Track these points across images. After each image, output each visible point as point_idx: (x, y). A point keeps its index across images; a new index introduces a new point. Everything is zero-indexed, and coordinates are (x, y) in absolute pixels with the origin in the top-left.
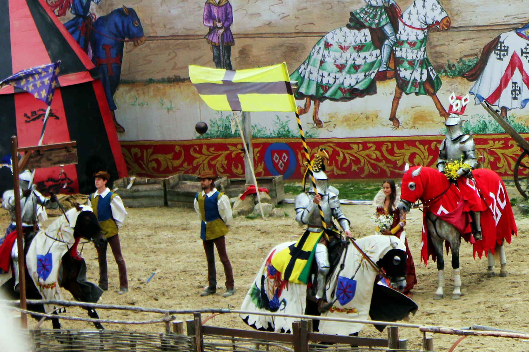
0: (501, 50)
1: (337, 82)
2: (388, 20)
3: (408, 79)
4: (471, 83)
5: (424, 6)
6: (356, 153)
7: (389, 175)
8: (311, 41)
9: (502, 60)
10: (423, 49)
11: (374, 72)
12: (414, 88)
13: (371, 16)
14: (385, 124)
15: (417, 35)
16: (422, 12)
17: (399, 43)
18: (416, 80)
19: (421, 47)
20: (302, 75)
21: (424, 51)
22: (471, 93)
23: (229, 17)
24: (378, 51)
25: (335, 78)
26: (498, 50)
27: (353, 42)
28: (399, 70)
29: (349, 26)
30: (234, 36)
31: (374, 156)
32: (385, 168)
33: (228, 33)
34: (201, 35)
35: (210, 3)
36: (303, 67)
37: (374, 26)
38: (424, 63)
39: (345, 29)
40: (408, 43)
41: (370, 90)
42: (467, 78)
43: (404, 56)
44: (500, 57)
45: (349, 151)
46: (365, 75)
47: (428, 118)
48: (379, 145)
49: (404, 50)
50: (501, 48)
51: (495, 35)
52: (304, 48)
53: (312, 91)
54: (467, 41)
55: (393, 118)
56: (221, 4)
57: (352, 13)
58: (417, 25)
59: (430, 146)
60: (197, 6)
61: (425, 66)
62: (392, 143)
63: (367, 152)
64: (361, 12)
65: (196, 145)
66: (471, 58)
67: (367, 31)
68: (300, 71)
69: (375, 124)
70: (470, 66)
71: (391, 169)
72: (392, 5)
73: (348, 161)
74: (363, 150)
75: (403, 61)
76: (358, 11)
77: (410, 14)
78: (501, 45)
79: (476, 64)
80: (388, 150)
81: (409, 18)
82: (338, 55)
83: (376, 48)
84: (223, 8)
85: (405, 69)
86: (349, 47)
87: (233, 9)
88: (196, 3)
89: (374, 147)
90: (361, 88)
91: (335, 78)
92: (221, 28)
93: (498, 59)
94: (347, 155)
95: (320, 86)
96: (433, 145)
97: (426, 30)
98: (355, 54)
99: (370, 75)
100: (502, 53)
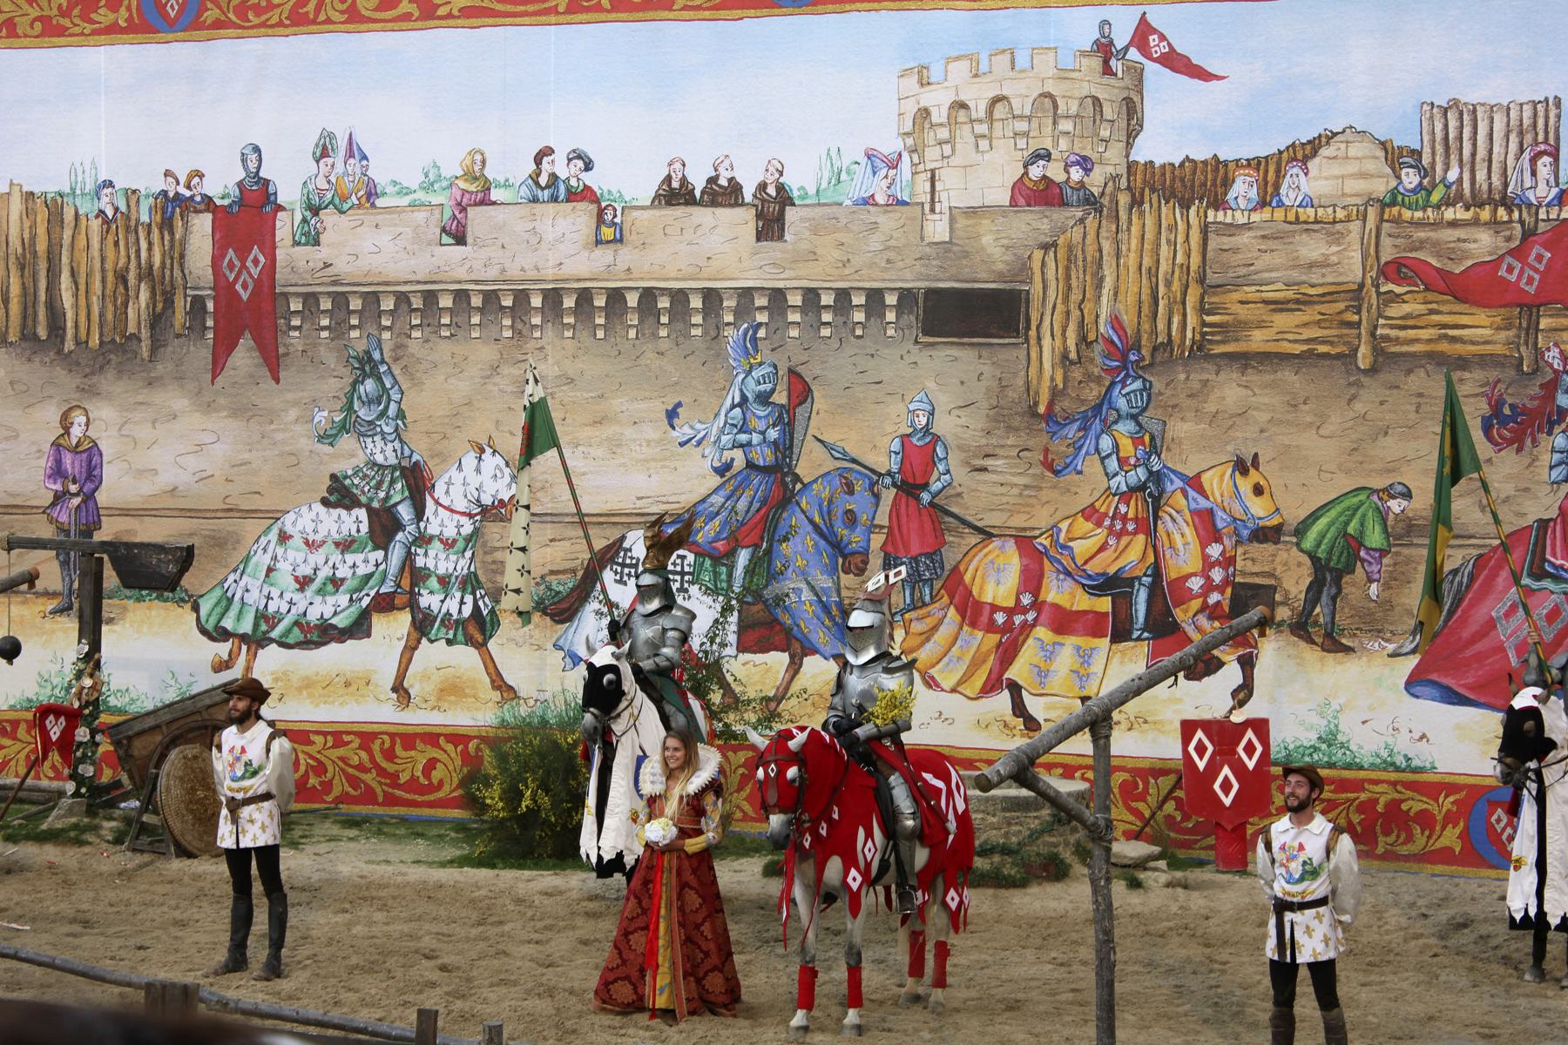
0: (623, 565)
1: (294, 610)
2: (407, 493)
3: (436, 612)
4: (560, 626)
5: (478, 471)
6: (319, 752)
7: (381, 799)
8: (252, 527)
9: (625, 584)
10: (468, 554)
11: (368, 595)
12: (444, 630)
13: (373, 483)
14: (382, 697)
15: (459, 526)
16: (474, 480)
17: (423, 540)
18: (451, 615)
19: (465, 550)
20: (229, 594)
21: (472, 559)
22: (557, 647)
23: (95, 473)
24: (380, 554)
25: (291, 603)
26: (618, 564)
27: (334, 532)
28: (419, 594)
29: (325, 502)
30: (102, 512)
31: (355, 761)
32: (374, 785)
33: (91, 504)
34: (37, 507)
35: (60, 445)
36: (231, 578)
37: (375, 504)
38: (470, 583)
39: (318, 507)
40: (441, 541)
41: (359, 628)
42: (552, 617)
43: (431, 565)
44: (621, 577)
45: (306, 748)
46: (351, 599)
47: (467, 691)
48: (367, 738)
49: (431, 553)
50: (624, 560)
51: (615, 534)
52: (238, 542)
53: (246, 627)
54: (557, 543)
55: (399, 688)
56: (80, 449)
57: (333, 477)
58: (461, 505)
59: (466, 747)
60: (35, 449)
61: (470, 590)
62: (392, 736)
63: (341, 752)
64: (356, 474)
65: (7, 721)
66: (560, 576)
67: (362, 513)
68: (226, 586)
69: (363, 696)
70: (560, 592)
71: (386, 788)
72: (417, 463)
73: (303, 768)
74: (334, 747)
75: (429, 576)
76: (350, 472)
77: (449, 484)
78: (625, 555)
79: (573, 590)
80: (382, 751)
81: (447, 492)
82: (300, 557)
83: (376, 547)
84: (84, 456)
85: (431, 592)
86: (324, 542)
87: (105, 459)
88: (33, 443)
89: (357, 742)
90: (340, 626)
91: (291, 603)
92: (77, 495)
93: (616, 581)
94: (301, 756)
95: (262, 616)
96: (472, 745)
97: (478, 518)
98: (336, 557)
99: (361, 600)
100: (626, 570)
